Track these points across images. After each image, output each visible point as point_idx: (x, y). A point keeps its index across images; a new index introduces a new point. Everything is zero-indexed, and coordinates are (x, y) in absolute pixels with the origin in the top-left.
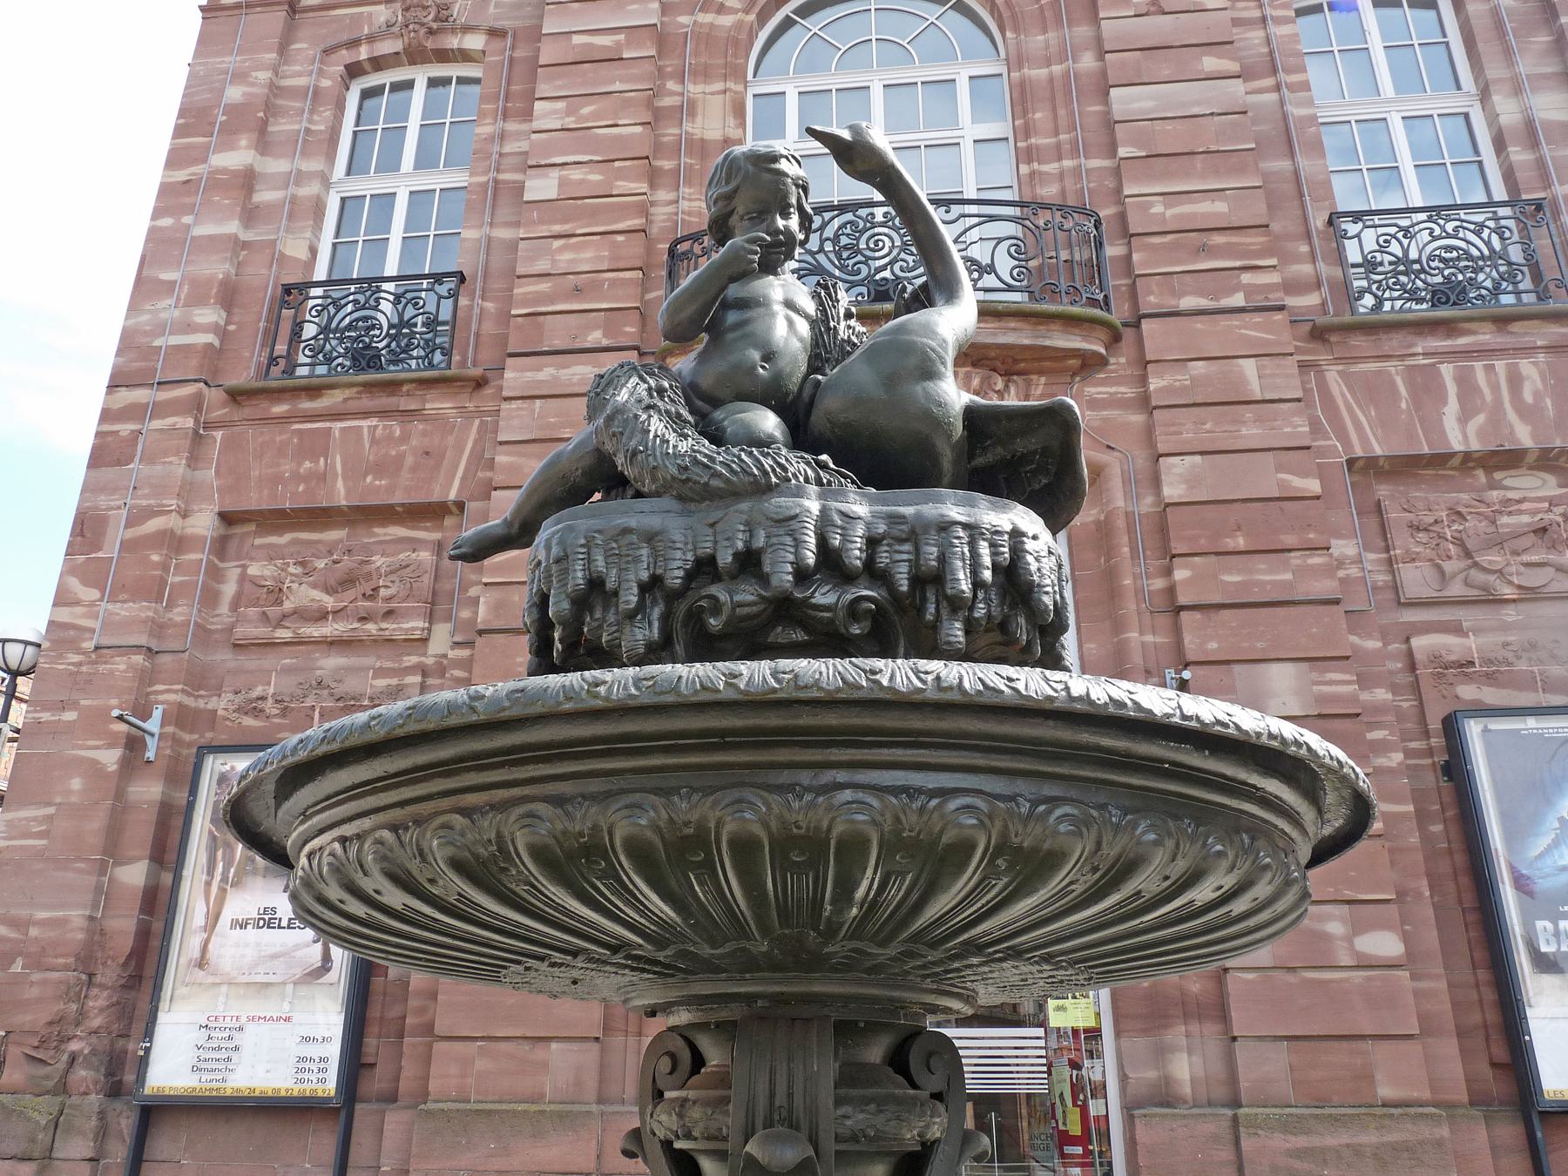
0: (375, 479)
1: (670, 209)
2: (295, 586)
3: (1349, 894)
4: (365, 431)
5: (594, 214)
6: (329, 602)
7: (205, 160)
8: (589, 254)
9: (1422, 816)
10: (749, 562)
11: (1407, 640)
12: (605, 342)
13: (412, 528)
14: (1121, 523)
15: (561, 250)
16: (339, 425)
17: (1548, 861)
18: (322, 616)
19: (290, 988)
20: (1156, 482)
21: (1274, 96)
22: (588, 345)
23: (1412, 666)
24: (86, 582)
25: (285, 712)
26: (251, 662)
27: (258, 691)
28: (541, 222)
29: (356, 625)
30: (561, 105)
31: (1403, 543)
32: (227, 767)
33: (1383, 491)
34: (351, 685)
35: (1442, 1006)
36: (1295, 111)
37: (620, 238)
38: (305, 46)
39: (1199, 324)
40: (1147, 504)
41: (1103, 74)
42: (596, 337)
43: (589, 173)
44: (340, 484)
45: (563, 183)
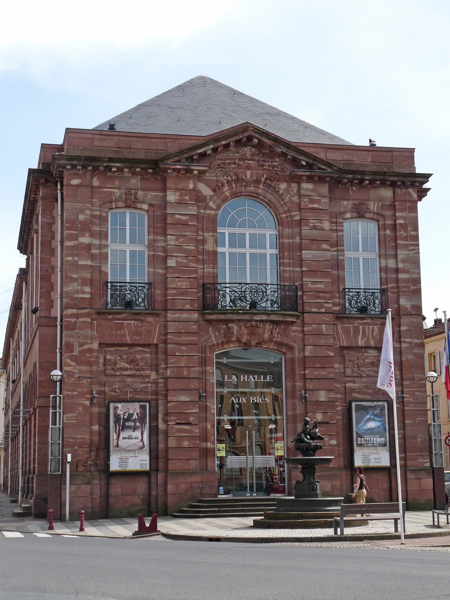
0: (136, 337)
1: (202, 270)
2: (120, 362)
3: (329, 434)
4: (132, 324)
5: (185, 272)
6: (128, 366)
7: (77, 239)
8: (185, 283)
9: (343, 419)
10: (310, 447)
11: (345, 384)
12: (190, 308)
13: (143, 348)
14: (297, 360)
15: (178, 281)
16: (125, 322)
17: (362, 428)
18: (127, 369)
19: (137, 451)
20: (304, 350)
21: (336, 253)
22: (186, 309)
23: (345, 389)
24: (72, 360)
25: (121, 392)
26: (110, 379)
27: (114, 387)
28: (172, 273)
29: (135, 372)
30: (174, 237)
31: (348, 364)
32: (116, 406)
33: (345, 352)
34: (135, 386)
35: (341, 452)
36: (340, 258)
37: (192, 280)
38: (97, 200)
39: (315, 315)
40: (301, 355)
41: (301, 243)
42: (188, 307)
43: (183, 260)
44: (128, 338)
45: (177, 262)
